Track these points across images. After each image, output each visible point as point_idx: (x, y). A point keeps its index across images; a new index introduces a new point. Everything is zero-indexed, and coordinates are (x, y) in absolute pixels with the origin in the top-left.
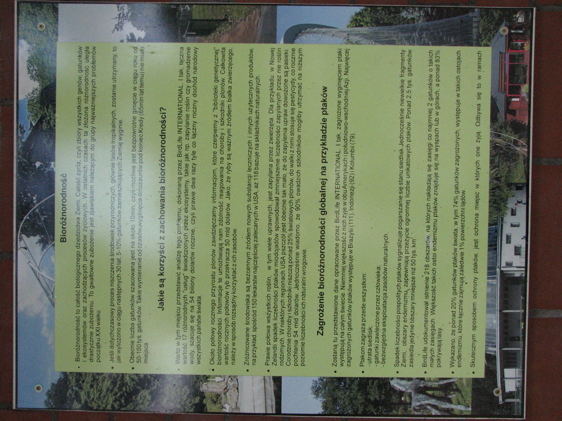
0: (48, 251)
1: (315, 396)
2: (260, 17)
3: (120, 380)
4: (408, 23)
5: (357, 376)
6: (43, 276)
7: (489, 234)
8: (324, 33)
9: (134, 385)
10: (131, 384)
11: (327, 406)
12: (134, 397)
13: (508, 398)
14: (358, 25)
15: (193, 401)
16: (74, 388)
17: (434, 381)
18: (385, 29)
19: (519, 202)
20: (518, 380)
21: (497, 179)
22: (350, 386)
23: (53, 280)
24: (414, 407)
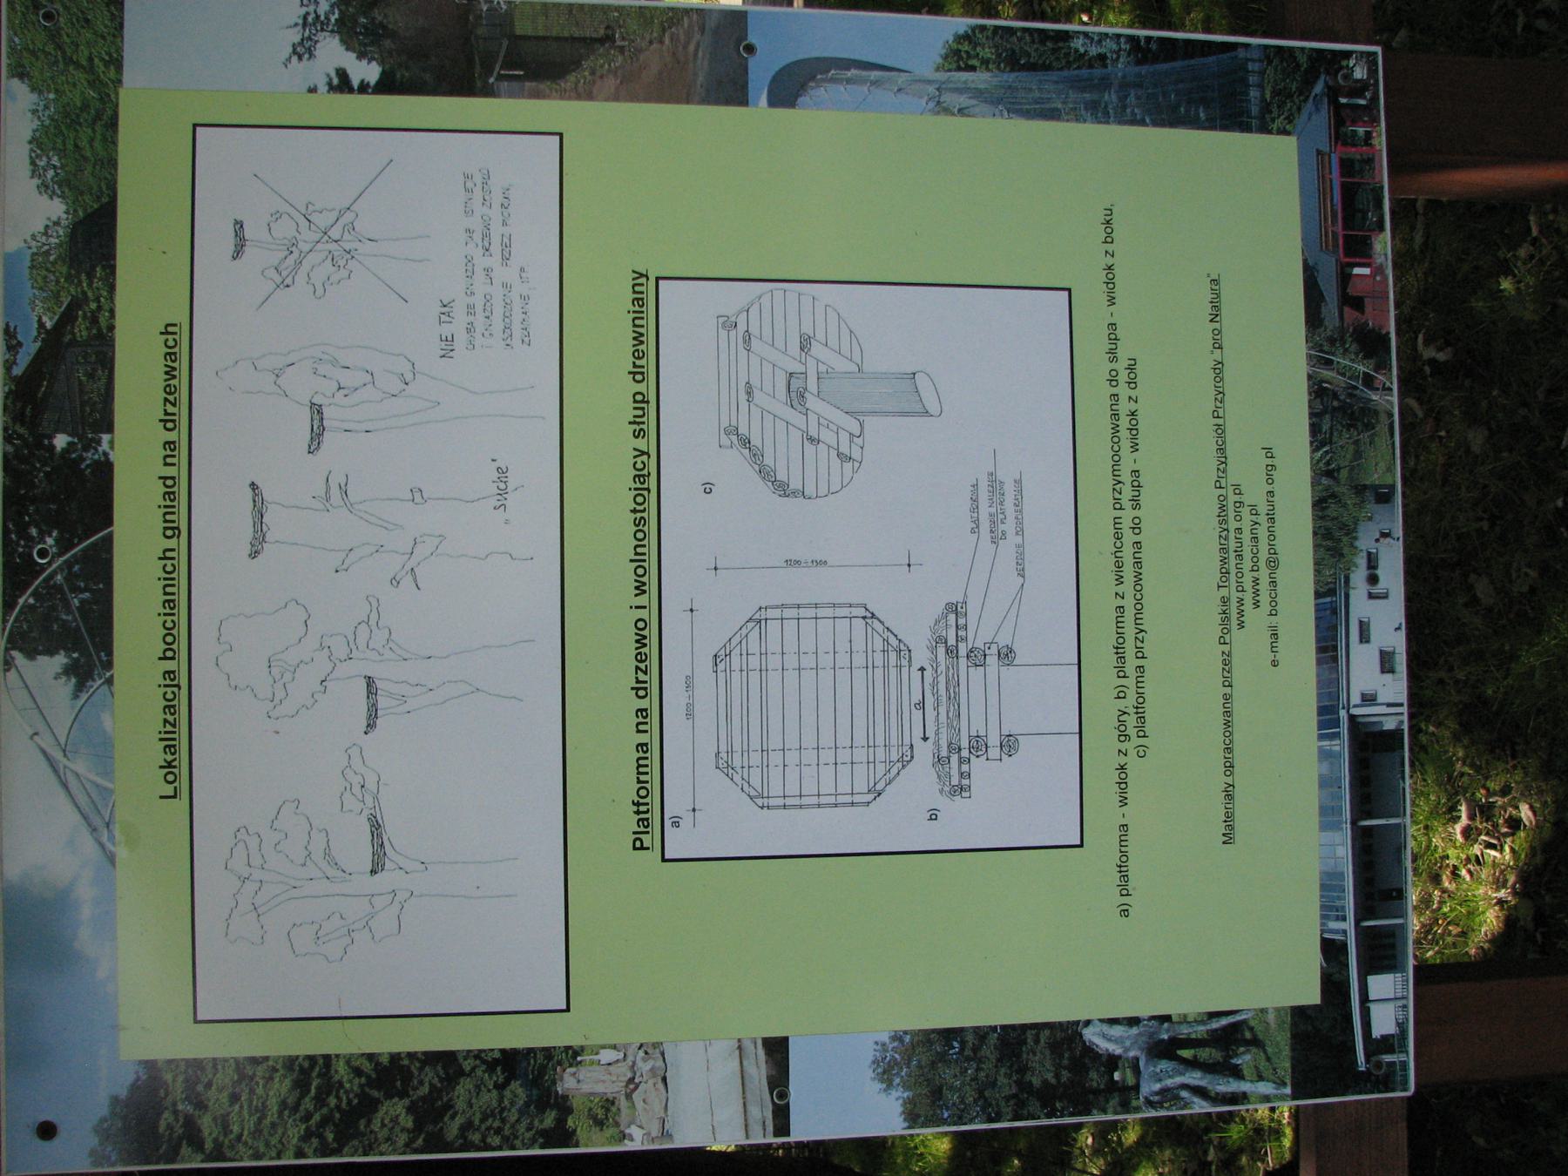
0: (92, 698)
1: (884, 1086)
2: (703, 33)
3: (319, 1075)
4: (1091, 66)
5: (993, 1024)
6: (77, 775)
7: (1318, 619)
8: (874, 83)
9: (361, 1086)
10: (352, 1084)
11: (916, 1111)
12: (362, 1123)
15: (536, 1123)
16: (180, 1107)
17: (1196, 1021)
19: (1385, 535)
20: (1400, 1003)
21: (1329, 474)
22: (975, 1050)
23: (110, 785)
24: (1146, 1098)
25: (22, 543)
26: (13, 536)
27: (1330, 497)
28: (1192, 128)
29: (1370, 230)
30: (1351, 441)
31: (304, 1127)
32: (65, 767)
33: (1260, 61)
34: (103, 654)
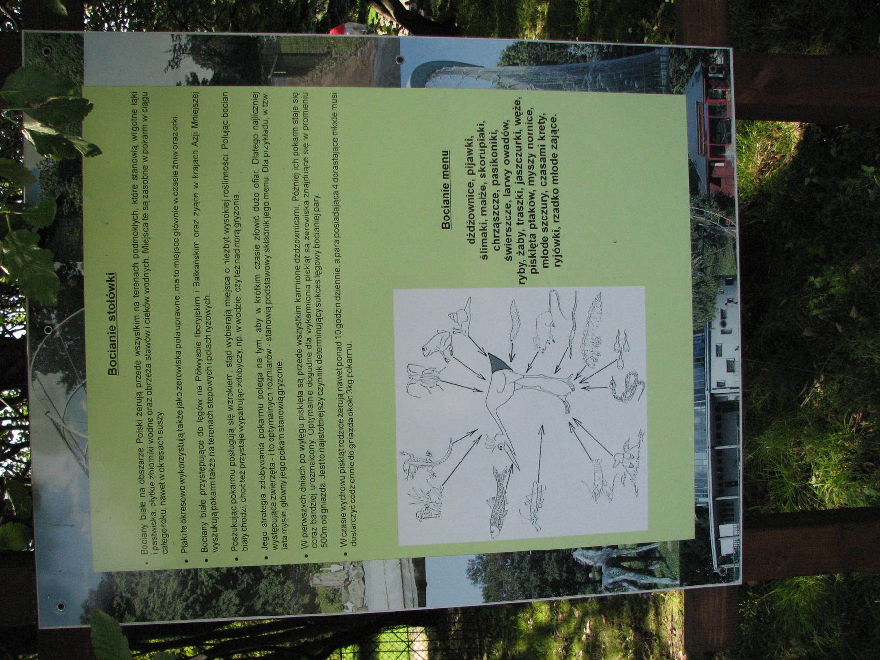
2: (377, 50)
3: (192, 579)
4: (578, 62)
5: (528, 550)
6: (70, 432)
7: (695, 345)
9: (213, 584)
10: (208, 583)
11: (490, 593)
12: (214, 602)
13: (725, 563)
14: (511, 63)
15: (300, 601)
16: (124, 595)
17: (630, 548)
18: (548, 70)
19: (730, 301)
21: (701, 270)
22: (520, 562)
25: (40, 317)
26: (35, 314)
27: (701, 282)
28: (631, 93)
29: (725, 143)
30: (712, 253)
31: (185, 603)
32: (63, 428)
33: (667, 56)
34: (81, 372)
